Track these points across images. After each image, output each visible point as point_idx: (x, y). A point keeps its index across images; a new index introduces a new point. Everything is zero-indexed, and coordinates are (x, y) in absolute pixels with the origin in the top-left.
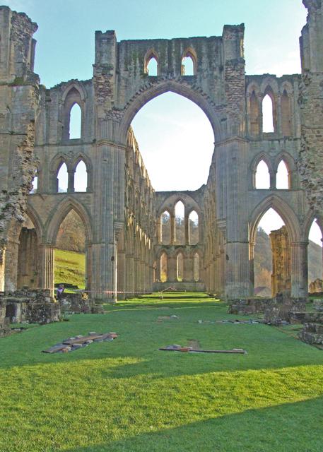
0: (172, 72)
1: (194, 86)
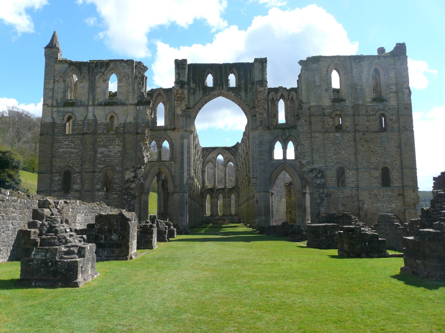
1: (236, 95)
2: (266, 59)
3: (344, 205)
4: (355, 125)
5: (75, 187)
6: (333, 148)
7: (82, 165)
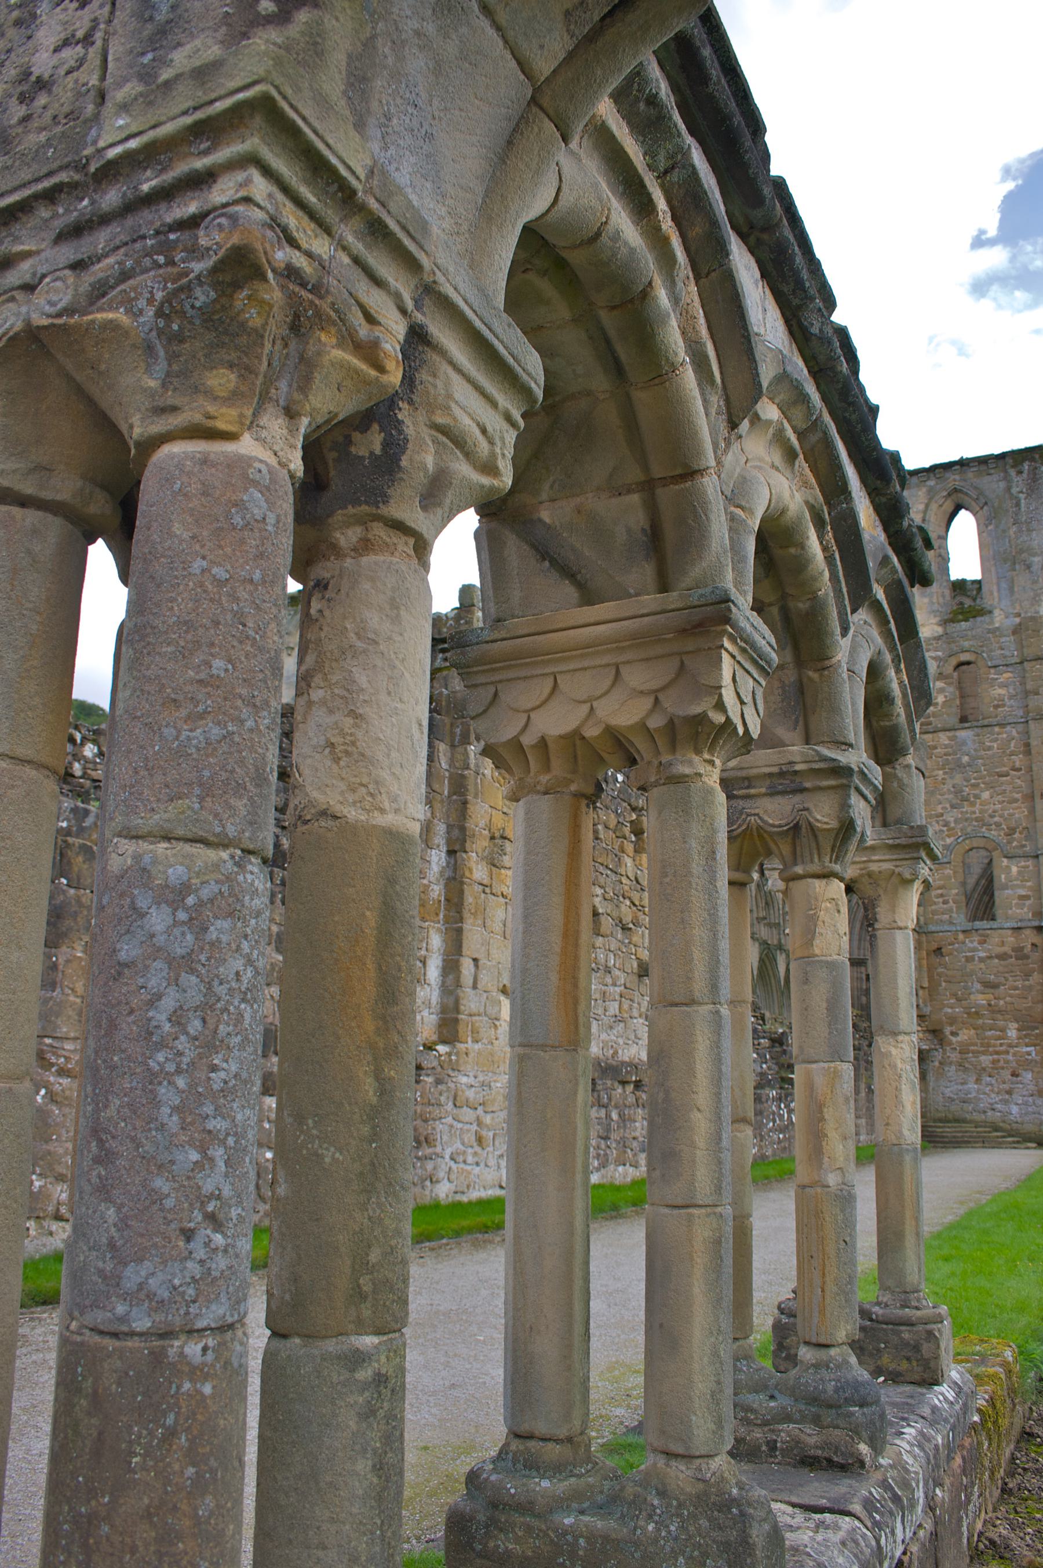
3: (990, 986)
6: (949, 784)
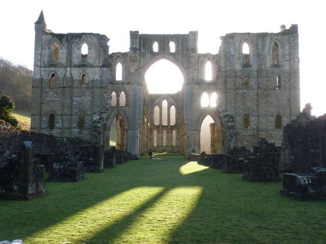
0: (165, 51)
2: (197, 32)
4: (258, 84)
5: (58, 125)
7: (62, 110)
